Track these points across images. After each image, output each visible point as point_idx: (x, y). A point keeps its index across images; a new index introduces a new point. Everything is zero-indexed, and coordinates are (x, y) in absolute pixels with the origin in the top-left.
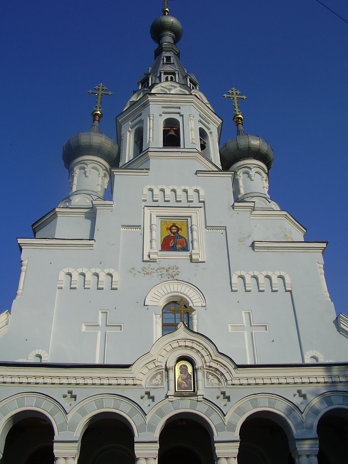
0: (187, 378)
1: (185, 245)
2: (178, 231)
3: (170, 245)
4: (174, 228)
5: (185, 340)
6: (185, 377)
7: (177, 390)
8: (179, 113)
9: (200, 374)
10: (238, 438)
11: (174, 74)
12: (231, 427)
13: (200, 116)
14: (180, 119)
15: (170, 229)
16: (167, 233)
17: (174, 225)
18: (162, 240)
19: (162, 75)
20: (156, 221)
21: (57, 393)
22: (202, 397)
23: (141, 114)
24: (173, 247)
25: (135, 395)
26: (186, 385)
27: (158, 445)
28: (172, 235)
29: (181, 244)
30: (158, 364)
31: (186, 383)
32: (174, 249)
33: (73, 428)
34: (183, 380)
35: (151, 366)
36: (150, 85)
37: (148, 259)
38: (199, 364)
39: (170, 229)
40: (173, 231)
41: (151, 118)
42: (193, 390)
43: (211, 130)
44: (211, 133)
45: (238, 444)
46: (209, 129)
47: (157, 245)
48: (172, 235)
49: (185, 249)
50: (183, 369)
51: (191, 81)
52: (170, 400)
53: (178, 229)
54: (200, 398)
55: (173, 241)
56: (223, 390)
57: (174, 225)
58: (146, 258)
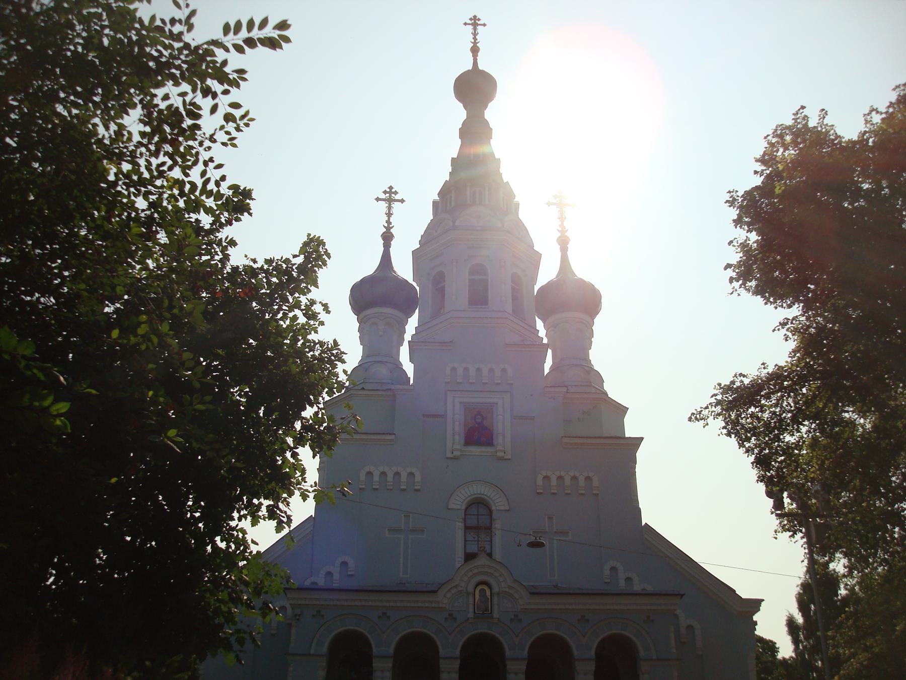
9: (495, 599)
27: (458, 662)
28: (477, 426)
30: (460, 589)
35: (454, 591)
36: (453, 204)
37: (452, 456)
38: (496, 589)
40: (477, 420)
48: (477, 426)
50: (482, 592)
58: (449, 455)
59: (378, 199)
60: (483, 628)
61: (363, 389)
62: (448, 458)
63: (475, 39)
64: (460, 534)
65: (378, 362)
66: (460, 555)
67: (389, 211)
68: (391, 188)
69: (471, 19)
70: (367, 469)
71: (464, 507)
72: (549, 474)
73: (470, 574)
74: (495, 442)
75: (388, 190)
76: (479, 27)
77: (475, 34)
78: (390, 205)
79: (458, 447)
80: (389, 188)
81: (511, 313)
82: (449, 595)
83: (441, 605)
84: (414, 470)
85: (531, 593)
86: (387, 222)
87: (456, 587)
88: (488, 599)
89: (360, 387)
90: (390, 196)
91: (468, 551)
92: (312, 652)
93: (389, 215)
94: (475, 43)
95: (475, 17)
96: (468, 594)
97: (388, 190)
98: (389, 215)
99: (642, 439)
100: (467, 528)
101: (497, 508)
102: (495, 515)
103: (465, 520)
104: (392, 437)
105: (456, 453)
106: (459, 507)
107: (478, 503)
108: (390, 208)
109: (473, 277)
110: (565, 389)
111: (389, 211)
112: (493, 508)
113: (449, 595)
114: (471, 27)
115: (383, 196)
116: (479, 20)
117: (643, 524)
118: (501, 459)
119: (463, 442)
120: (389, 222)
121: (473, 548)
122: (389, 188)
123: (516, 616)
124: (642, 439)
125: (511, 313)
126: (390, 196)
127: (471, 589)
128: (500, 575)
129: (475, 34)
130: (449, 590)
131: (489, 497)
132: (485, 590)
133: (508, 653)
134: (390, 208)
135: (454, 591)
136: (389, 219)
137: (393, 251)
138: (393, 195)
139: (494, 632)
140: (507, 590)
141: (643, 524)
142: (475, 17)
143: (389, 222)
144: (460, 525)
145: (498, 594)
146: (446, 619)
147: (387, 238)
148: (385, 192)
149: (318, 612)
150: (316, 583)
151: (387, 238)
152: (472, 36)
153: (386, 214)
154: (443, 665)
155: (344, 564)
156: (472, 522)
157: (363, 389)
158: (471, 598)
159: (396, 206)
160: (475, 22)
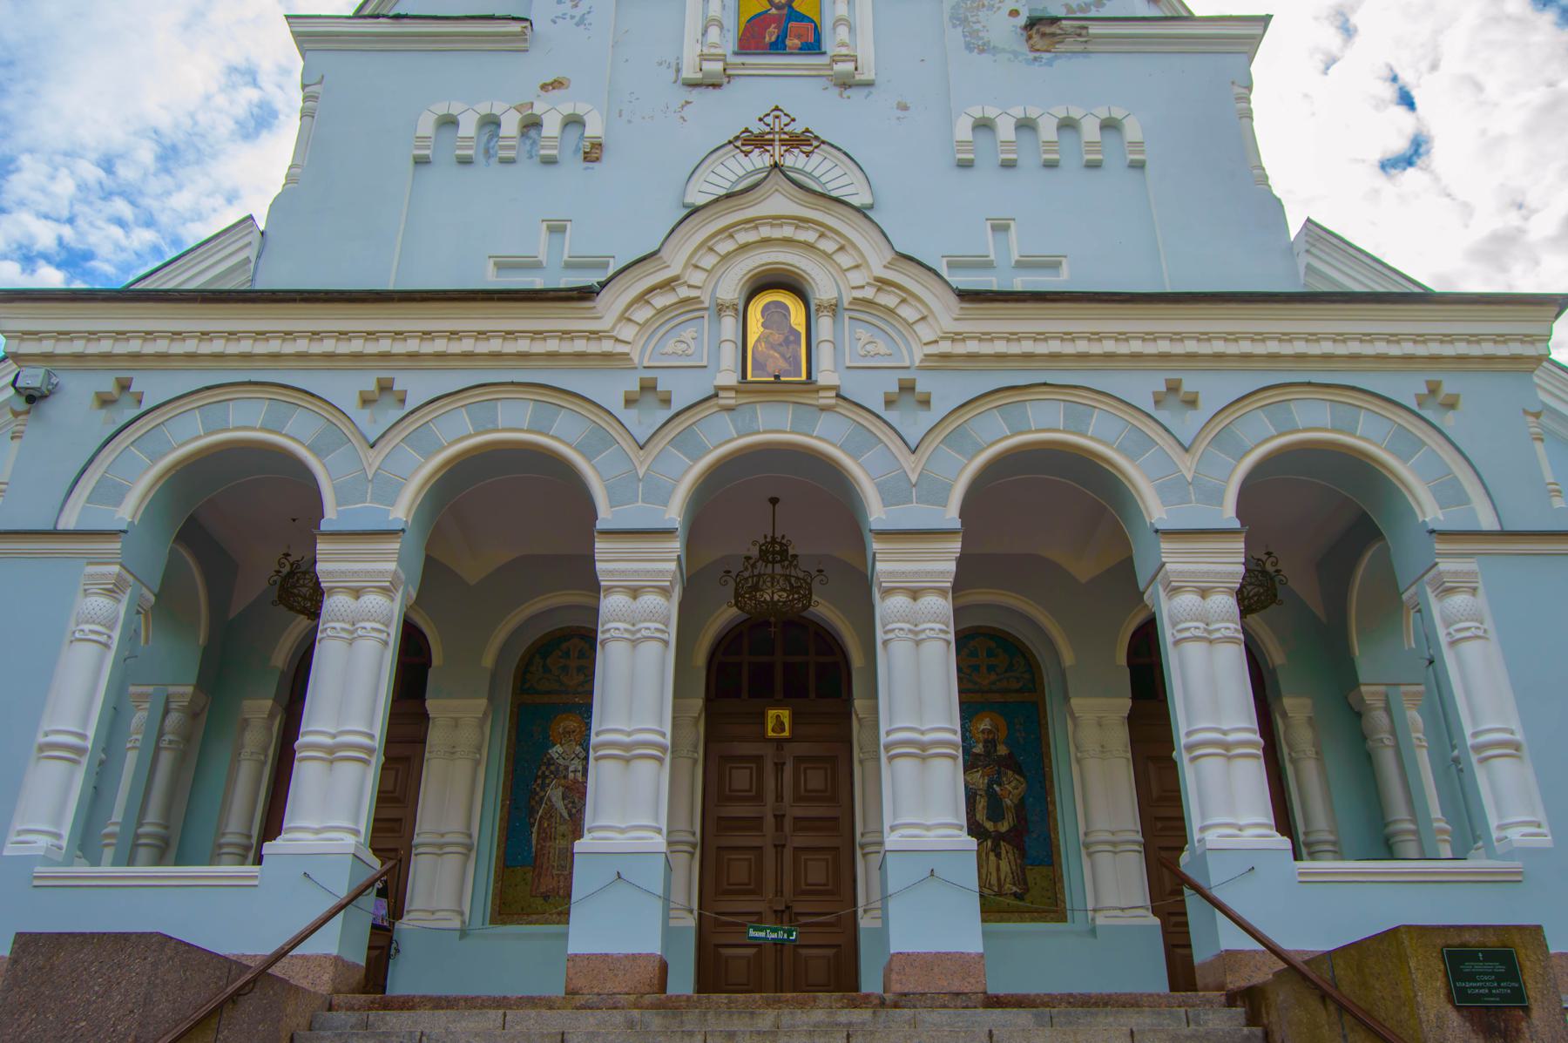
0: (787, 342)
1: (811, 38)
3: (767, 39)
5: (777, 220)
6: (778, 337)
7: (749, 378)
9: (824, 325)
10: (957, 524)
18: (742, 26)
22: (833, 394)
26: (783, 365)
29: (799, 37)
30: (684, 292)
31: (783, 356)
33: (388, 491)
35: (661, 301)
42: (804, 377)
45: (956, 546)
48: (774, 11)
50: (775, 315)
52: (722, 402)
54: (827, 399)
55: (775, 28)
56: (905, 375)
58: (689, 73)
73: (725, 247)
82: (642, 314)
83: (607, 346)
84: (581, 109)
87: (668, 285)
88: (799, 334)
92: (69, 521)
99: (1265, 20)
104: (516, 27)
124: (1265, 20)
128: (842, 248)
130: (643, 298)
132: (786, 308)
133: (878, 514)
140: (869, 293)
141: (1294, 227)
158: (729, 325)
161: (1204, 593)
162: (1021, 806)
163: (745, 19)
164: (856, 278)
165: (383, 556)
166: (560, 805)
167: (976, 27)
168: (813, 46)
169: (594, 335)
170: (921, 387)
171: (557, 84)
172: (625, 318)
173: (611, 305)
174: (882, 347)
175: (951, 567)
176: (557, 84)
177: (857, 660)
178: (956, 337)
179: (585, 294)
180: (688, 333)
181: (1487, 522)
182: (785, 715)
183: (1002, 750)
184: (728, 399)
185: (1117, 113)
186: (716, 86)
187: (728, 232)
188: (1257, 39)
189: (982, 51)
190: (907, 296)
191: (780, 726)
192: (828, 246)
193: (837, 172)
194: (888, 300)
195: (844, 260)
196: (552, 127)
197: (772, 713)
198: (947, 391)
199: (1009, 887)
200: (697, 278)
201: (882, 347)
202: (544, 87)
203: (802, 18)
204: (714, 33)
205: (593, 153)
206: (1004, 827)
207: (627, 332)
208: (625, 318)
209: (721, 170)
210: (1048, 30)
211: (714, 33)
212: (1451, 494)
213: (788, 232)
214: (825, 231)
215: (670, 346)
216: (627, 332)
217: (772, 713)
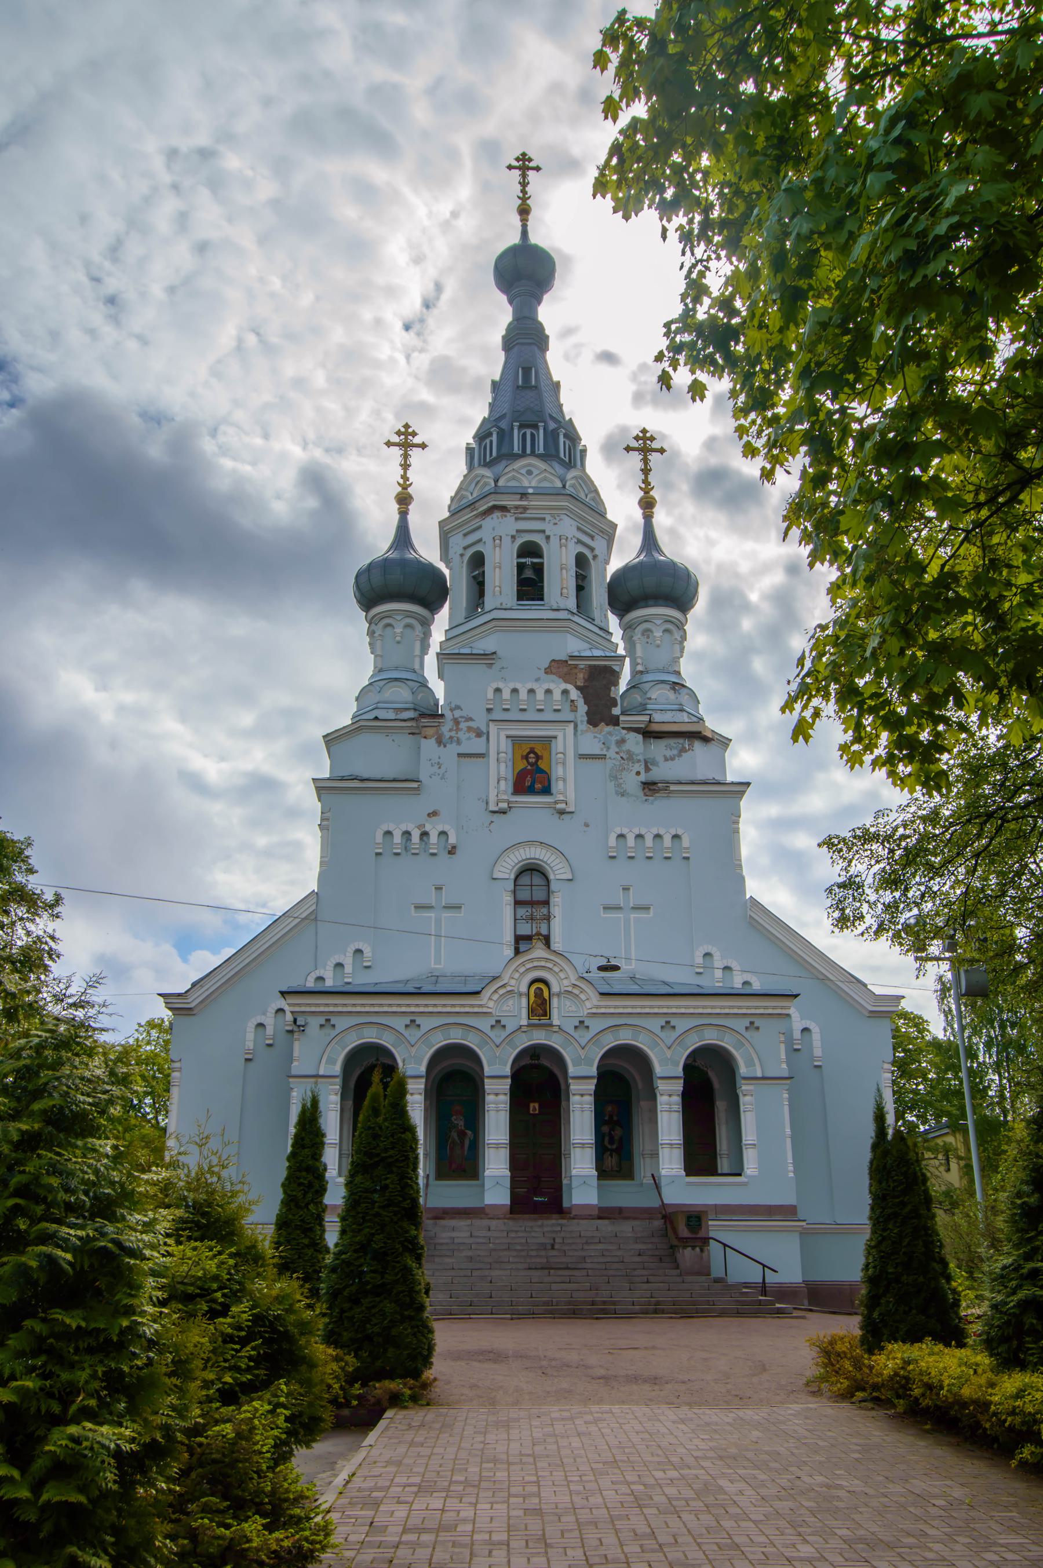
2: (537, 761)
4: (532, 755)
5: (539, 959)
6: (540, 1002)
8: (543, 531)
9: (555, 1001)
11: (535, 427)
12: (589, 1062)
13: (579, 529)
14: (542, 542)
15: (526, 757)
16: (522, 765)
17: (532, 751)
19: (516, 431)
20: (505, 745)
21: (399, 1023)
23: (480, 527)
24: (529, 787)
25: (484, 1024)
27: (509, 1081)
29: (541, 783)
30: (509, 988)
32: (531, 791)
34: (538, 1005)
35: (502, 991)
36: (494, 454)
37: (496, 809)
38: (555, 988)
39: (526, 757)
41: (497, 542)
43: (597, 552)
44: (595, 557)
45: (595, 1081)
46: (592, 549)
47: (507, 786)
49: (547, 791)
51: (566, 436)
53: (538, 757)
54: (556, 1029)
57: (532, 751)
58: (493, 807)
59: (389, 444)
60: (539, 1038)
61: (376, 718)
62: (494, 812)
63: (524, 192)
64: (508, 912)
65: (396, 679)
66: (509, 937)
67: (406, 461)
68: (407, 426)
69: (517, 159)
70: (385, 827)
71: (513, 876)
72: (625, 831)
73: (522, 970)
74: (554, 790)
75: (403, 430)
76: (530, 173)
77: (524, 184)
78: (406, 451)
79: (505, 797)
80: (404, 427)
81: (575, 611)
82: (496, 997)
83: (485, 1010)
84: (446, 828)
85: (602, 994)
86: (402, 477)
89: (371, 716)
90: (406, 439)
91: (518, 933)
92: (321, 1073)
93: (405, 466)
94: (524, 197)
95: (524, 155)
96: (521, 995)
97: (403, 430)
98: (405, 466)
99: (748, 784)
100: (518, 903)
101: (558, 877)
102: (553, 886)
103: (514, 892)
104: (415, 785)
105: (504, 805)
106: (506, 876)
107: (532, 870)
108: (406, 456)
109: (523, 560)
110: (647, 718)
111: (406, 461)
112: (552, 877)
113: (496, 997)
114: (517, 173)
115: (396, 439)
116: (530, 160)
117: (748, 897)
118: (562, 812)
119: (510, 789)
120: (405, 477)
121: (525, 929)
122: (404, 427)
123: (582, 1022)
124: (748, 784)
125: (575, 611)
126: (406, 439)
127: (524, 989)
129: (524, 184)
130: (495, 991)
131: (545, 863)
134: (406, 456)
135: (502, 991)
136: (405, 473)
137: (412, 518)
138: (410, 437)
139: (555, 1041)
140: (570, 989)
141: (748, 897)
142: (524, 155)
143: (405, 477)
144: (509, 899)
145: (558, 995)
146: (492, 1027)
147: (404, 500)
148: (399, 433)
149: (328, 1020)
150: (320, 979)
151: (404, 500)
152: (519, 188)
153: (401, 465)
154: (489, 1085)
155: (359, 951)
156: (524, 895)
157: (376, 718)
158: (524, 1001)
159: (415, 454)
160: (524, 165)
161: (670, 1096)
162: (621, 1139)
163: (516, 773)
164: (566, 982)
165: (419, 1083)
166: (456, 1138)
167: (621, 781)
168: (547, 791)
169: (481, 1006)
170: (586, 1024)
171: (434, 814)
172: (490, 999)
173: (487, 994)
174: (573, 1008)
175: (593, 1087)
176: (434, 814)
177: (563, 1087)
178: (597, 1007)
179: (478, 993)
180: (511, 1002)
181: (759, 1075)
182: (537, 1105)
183: (615, 1118)
184: (524, 1029)
185: (680, 832)
186: (504, 813)
187: (523, 964)
188: (744, 792)
189: (623, 795)
190: (582, 991)
191: (535, 1109)
192: (556, 969)
193: (558, 861)
194: (576, 991)
195: (562, 975)
196: (433, 838)
197: (532, 1105)
198: (596, 1025)
199: (615, 1168)
200: (513, 982)
201: (573, 1008)
202: (429, 815)
203: (542, 771)
204: (503, 783)
205: (452, 851)
206: (614, 1147)
207: (491, 1004)
208: (490, 999)
209: (507, 859)
210: (652, 787)
211: (503, 783)
212: (750, 1063)
213: (543, 964)
214: (556, 964)
215: (505, 1008)
216: (491, 1004)
217: (532, 1105)
